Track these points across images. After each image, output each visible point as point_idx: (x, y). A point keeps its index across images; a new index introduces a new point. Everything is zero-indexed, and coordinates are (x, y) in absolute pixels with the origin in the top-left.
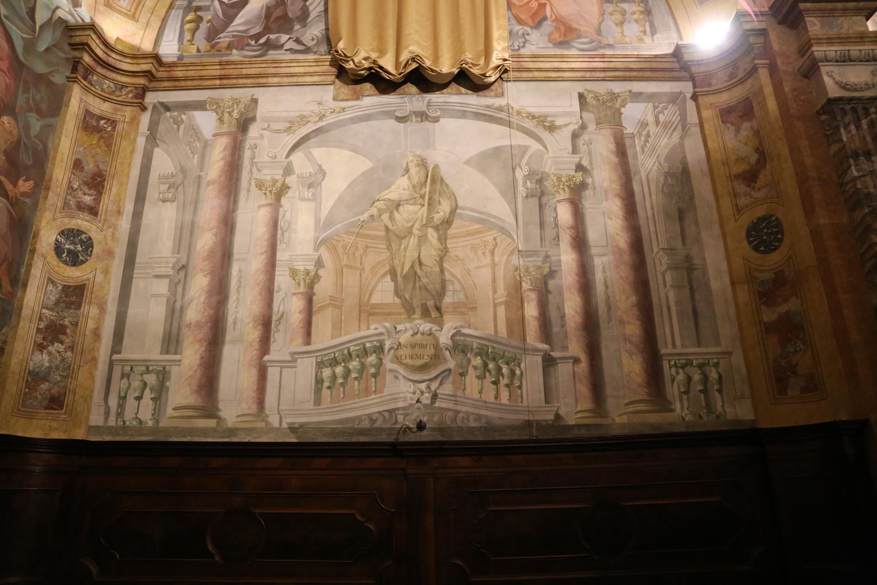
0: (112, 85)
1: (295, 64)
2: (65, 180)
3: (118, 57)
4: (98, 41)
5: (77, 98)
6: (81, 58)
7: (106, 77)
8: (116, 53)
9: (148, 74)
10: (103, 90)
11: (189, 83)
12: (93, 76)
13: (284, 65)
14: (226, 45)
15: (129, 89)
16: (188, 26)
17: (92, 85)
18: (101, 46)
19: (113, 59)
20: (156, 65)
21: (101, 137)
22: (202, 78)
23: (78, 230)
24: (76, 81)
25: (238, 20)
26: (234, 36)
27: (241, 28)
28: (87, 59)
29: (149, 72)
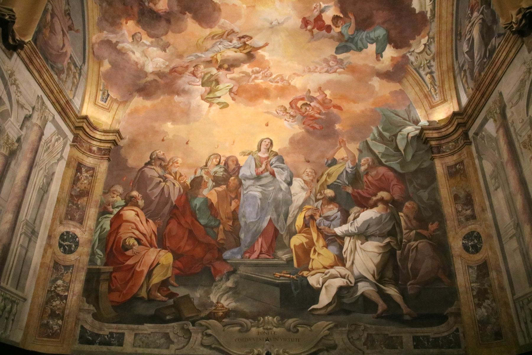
0: (453, 143)
1: (500, 54)
2: (454, 210)
3: (445, 129)
4: (431, 132)
5: (439, 165)
6: (431, 145)
7: (448, 143)
8: (443, 128)
9: (459, 125)
10: (451, 150)
11: (476, 112)
12: (443, 147)
13: (497, 60)
14: (478, 75)
15: (460, 138)
16: (464, 80)
17: (444, 152)
18: (434, 132)
19: (444, 132)
20: (460, 117)
21: (461, 174)
22: (477, 105)
23: (471, 232)
24: (434, 158)
25: (476, 55)
26: (478, 65)
27: (478, 57)
28: (433, 143)
29: (458, 124)
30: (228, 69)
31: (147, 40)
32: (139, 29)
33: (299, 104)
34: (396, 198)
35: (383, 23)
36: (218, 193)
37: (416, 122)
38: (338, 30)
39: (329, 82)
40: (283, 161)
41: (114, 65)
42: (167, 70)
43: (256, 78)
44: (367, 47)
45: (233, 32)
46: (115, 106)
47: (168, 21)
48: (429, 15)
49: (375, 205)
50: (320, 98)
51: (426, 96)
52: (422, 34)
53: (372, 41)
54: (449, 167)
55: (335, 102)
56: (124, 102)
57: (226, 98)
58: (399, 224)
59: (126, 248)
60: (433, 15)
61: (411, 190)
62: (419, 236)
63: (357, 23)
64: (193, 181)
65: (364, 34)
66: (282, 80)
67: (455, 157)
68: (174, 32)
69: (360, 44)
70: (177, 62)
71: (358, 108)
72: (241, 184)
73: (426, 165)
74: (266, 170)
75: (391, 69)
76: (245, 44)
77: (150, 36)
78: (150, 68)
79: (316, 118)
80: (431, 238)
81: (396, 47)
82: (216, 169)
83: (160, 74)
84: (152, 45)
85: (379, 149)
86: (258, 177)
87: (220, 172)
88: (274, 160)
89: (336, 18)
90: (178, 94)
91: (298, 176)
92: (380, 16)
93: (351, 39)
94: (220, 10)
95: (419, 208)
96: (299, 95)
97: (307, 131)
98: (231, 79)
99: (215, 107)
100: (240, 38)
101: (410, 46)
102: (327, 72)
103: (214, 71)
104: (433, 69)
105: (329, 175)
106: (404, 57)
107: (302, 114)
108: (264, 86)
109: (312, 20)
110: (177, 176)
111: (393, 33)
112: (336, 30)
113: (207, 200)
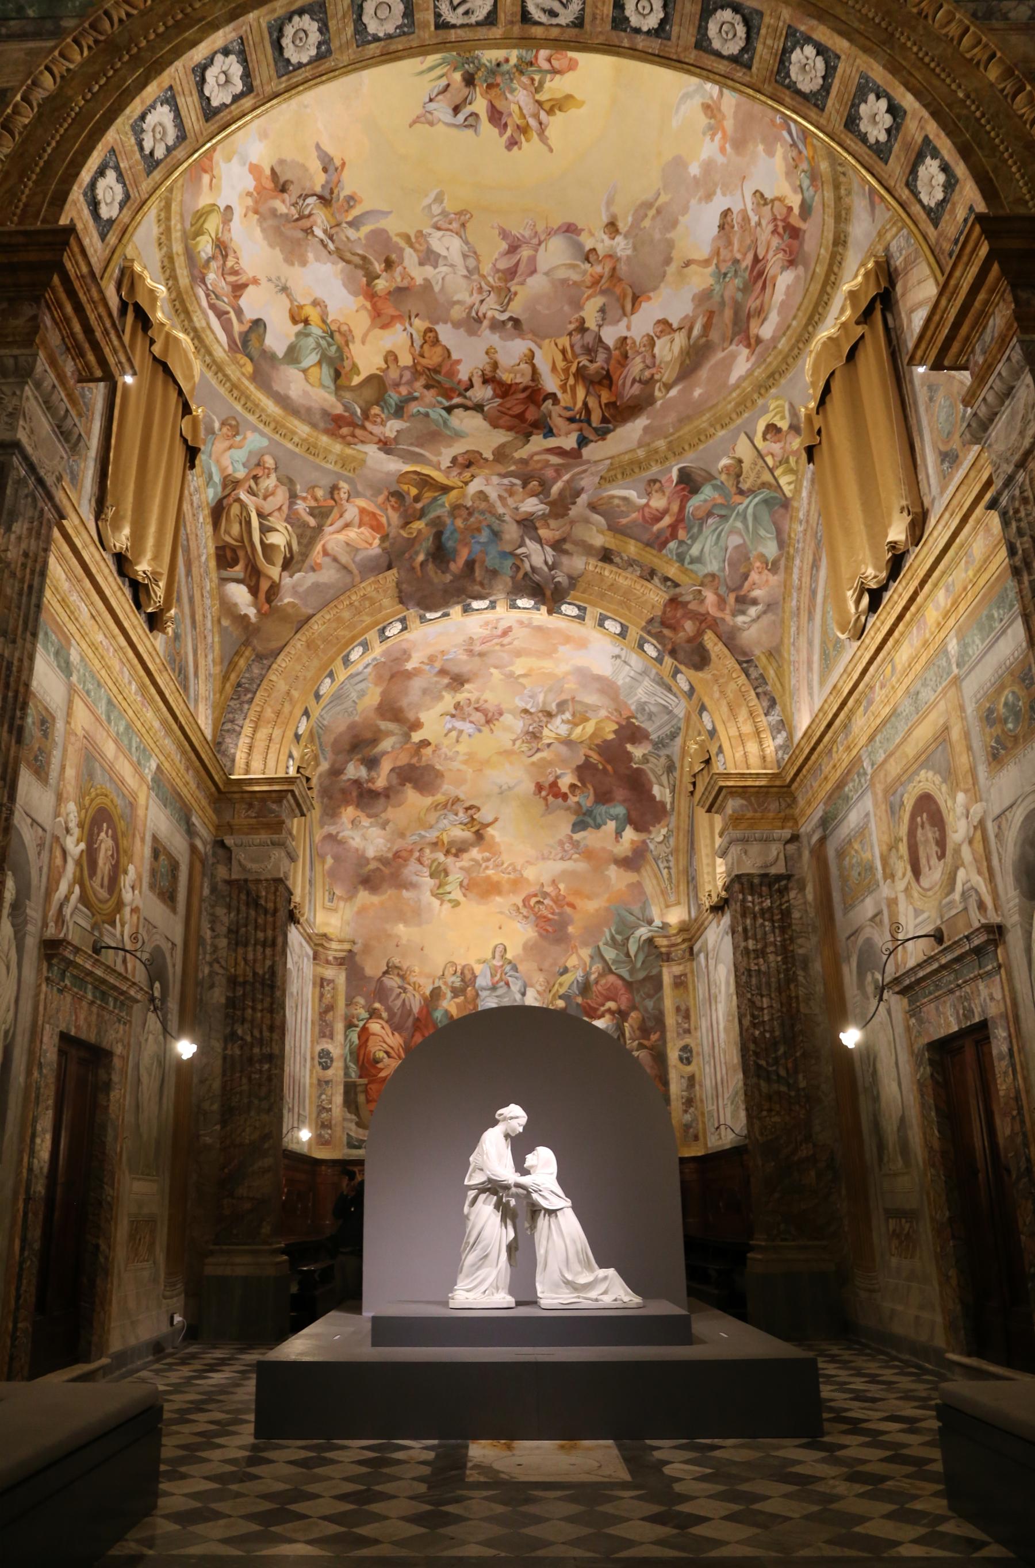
30: (456, 855)
31: (366, 822)
32: (359, 813)
33: (533, 901)
34: (623, 1007)
35: (624, 801)
36: (458, 1005)
37: (650, 922)
38: (576, 799)
39: (564, 873)
40: (516, 971)
41: (336, 858)
42: (390, 855)
43: (487, 868)
44: (605, 824)
45: (457, 800)
46: (342, 904)
47: (387, 797)
48: (668, 807)
49: (602, 1016)
50: (553, 894)
51: (662, 893)
52: (663, 823)
53: (615, 818)
54: (675, 977)
55: (570, 899)
56: (351, 897)
57: (457, 894)
58: (623, 1034)
59: (377, 1061)
60: (673, 809)
61: (637, 999)
62: (641, 1046)
63: (596, 794)
64: (432, 992)
65: (603, 809)
66: (515, 870)
67: (681, 968)
68: (393, 806)
69: (599, 820)
70: (399, 844)
71: (591, 906)
72: (477, 995)
73: (654, 972)
74: (501, 980)
75: (630, 854)
76: (473, 819)
77: (369, 816)
78: (371, 853)
79: (549, 920)
80: (651, 1048)
81: (637, 829)
82: (454, 979)
83: (381, 860)
84: (372, 825)
85: (610, 954)
86: (494, 988)
87: (458, 983)
88: (508, 968)
89: (573, 787)
90: (407, 889)
91: (532, 986)
92: (620, 793)
93: (589, 813)
94: (442, 776)
95: (643, 1019)
96: (533, 890)
97: (541, 935)
98: (461, 868)
99: (447, 906)
100: (467, 809)
101: (650, 832)
102: (562, 859)
103: (441, 857)
104: (672, 864)
105: (561, 985)
106: (644, 842)
107: (535, 914)
108: (495, 878)
109: (547, 785)
110: (416, 987)
111: (634, 815)
112: (573, 800)
113: (447, 1012)
